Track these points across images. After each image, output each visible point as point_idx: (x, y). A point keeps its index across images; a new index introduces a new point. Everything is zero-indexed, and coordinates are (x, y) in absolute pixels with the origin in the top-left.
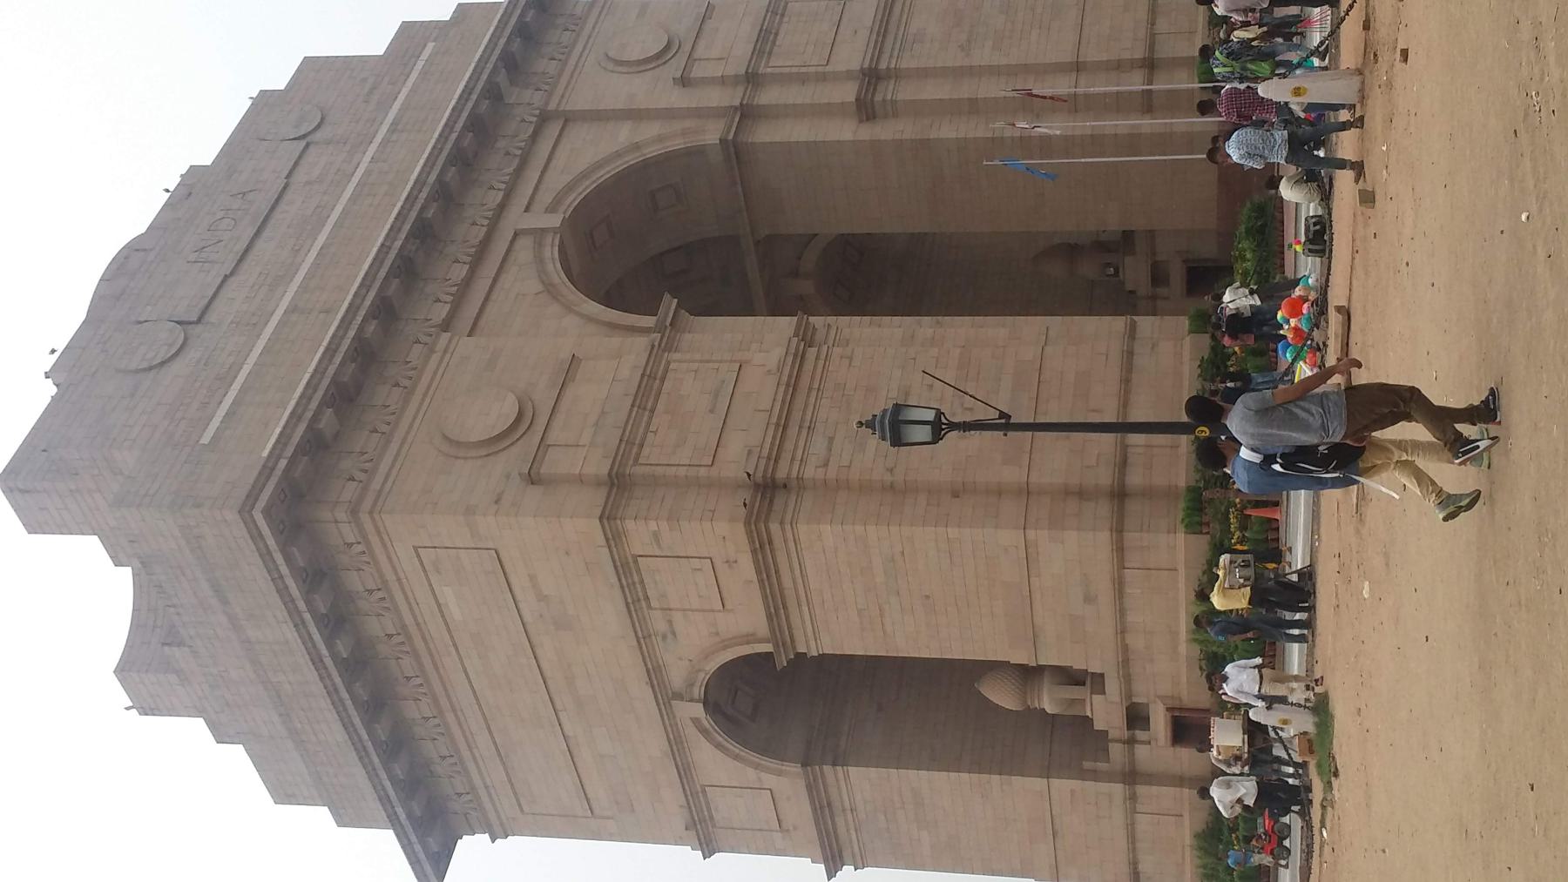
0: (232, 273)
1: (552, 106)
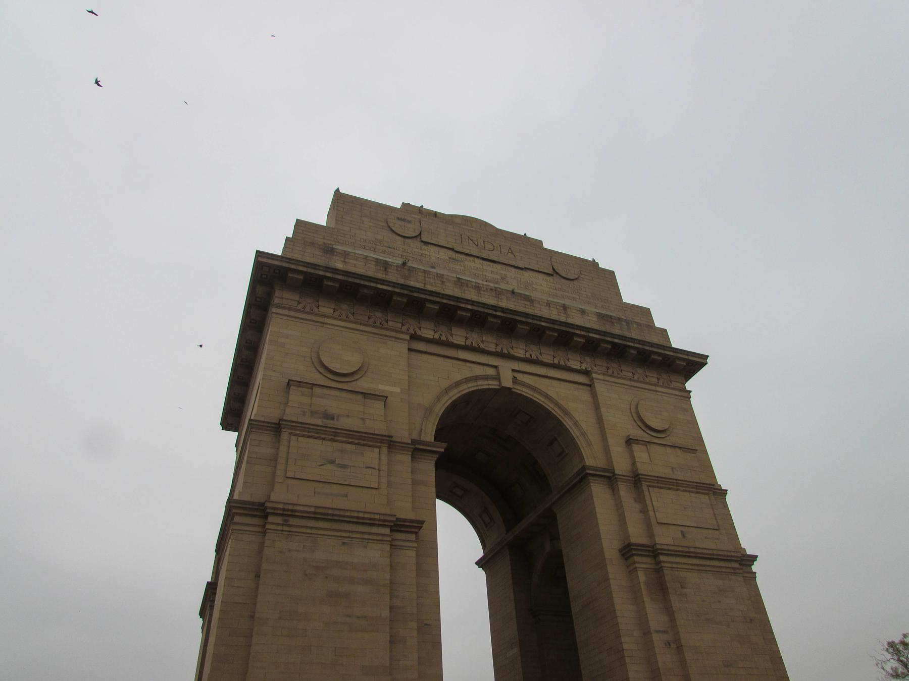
0: (457, 252)
1: (594, 375)
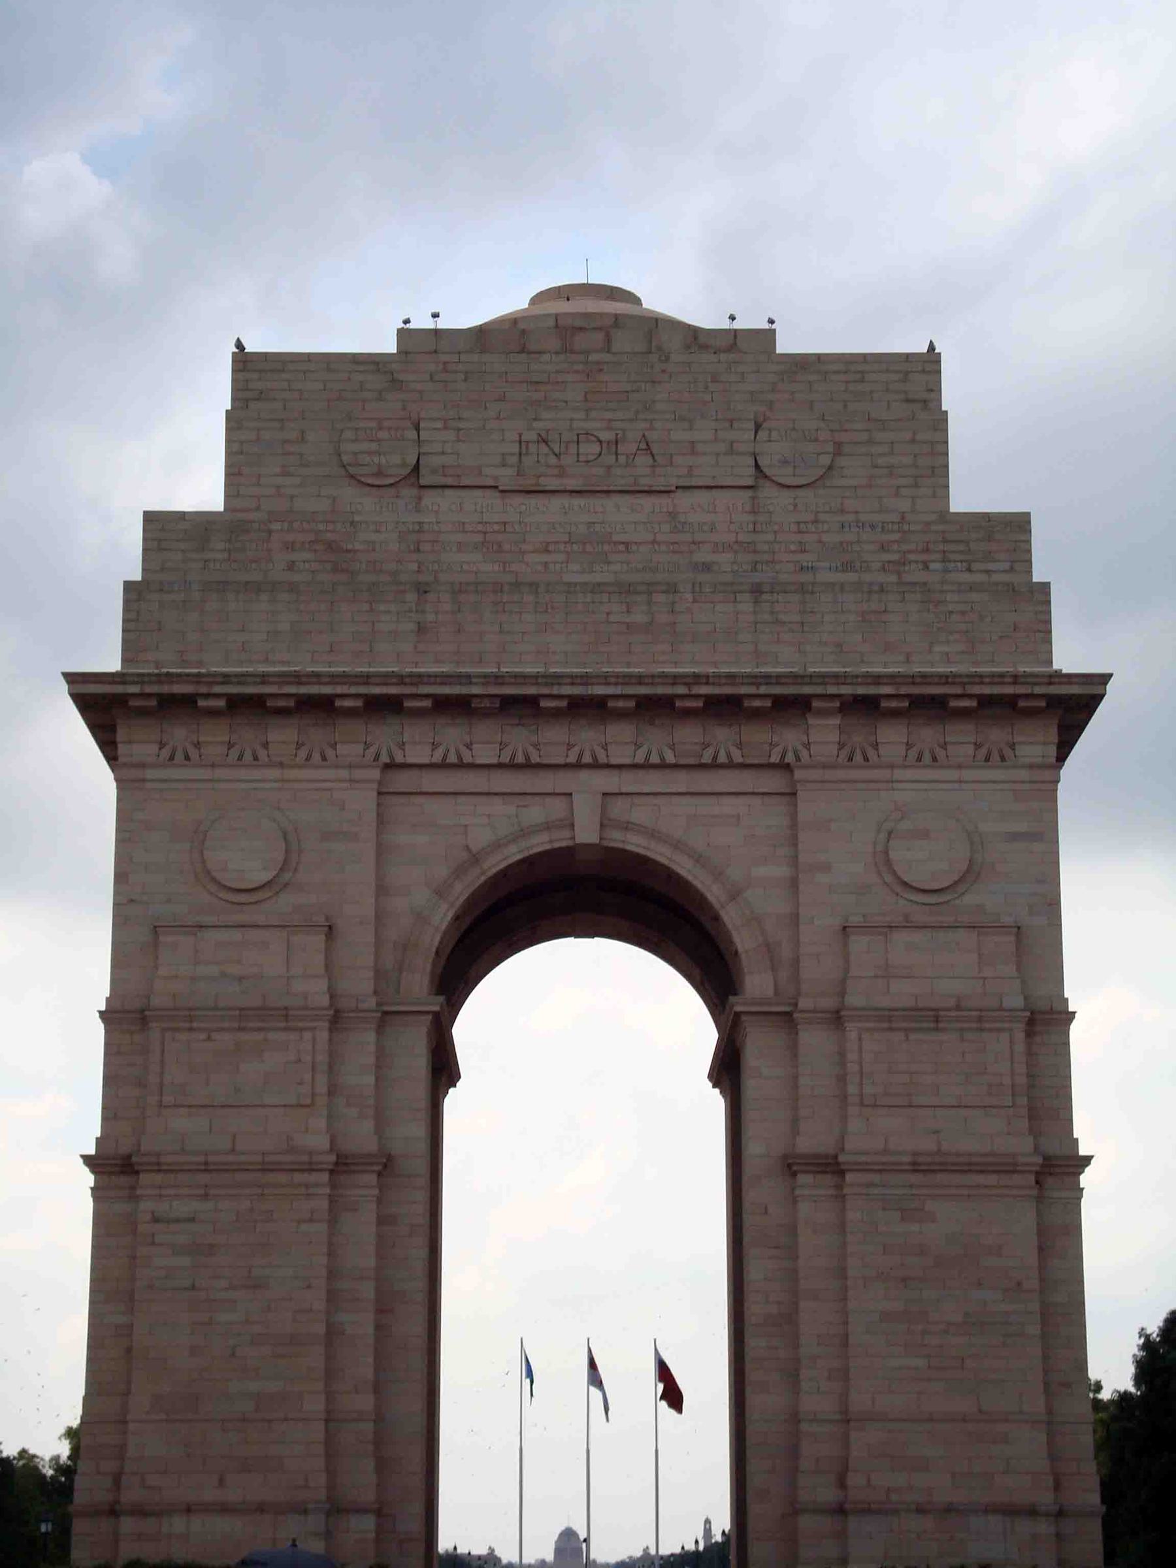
0: (502, 491)
1: (799, 774)
